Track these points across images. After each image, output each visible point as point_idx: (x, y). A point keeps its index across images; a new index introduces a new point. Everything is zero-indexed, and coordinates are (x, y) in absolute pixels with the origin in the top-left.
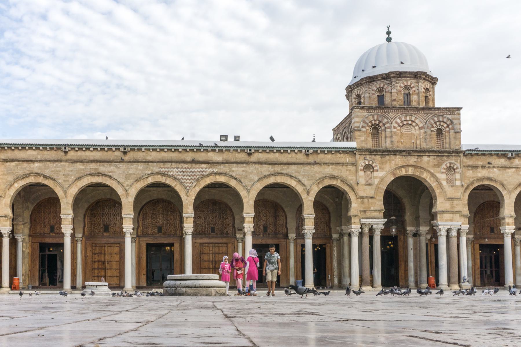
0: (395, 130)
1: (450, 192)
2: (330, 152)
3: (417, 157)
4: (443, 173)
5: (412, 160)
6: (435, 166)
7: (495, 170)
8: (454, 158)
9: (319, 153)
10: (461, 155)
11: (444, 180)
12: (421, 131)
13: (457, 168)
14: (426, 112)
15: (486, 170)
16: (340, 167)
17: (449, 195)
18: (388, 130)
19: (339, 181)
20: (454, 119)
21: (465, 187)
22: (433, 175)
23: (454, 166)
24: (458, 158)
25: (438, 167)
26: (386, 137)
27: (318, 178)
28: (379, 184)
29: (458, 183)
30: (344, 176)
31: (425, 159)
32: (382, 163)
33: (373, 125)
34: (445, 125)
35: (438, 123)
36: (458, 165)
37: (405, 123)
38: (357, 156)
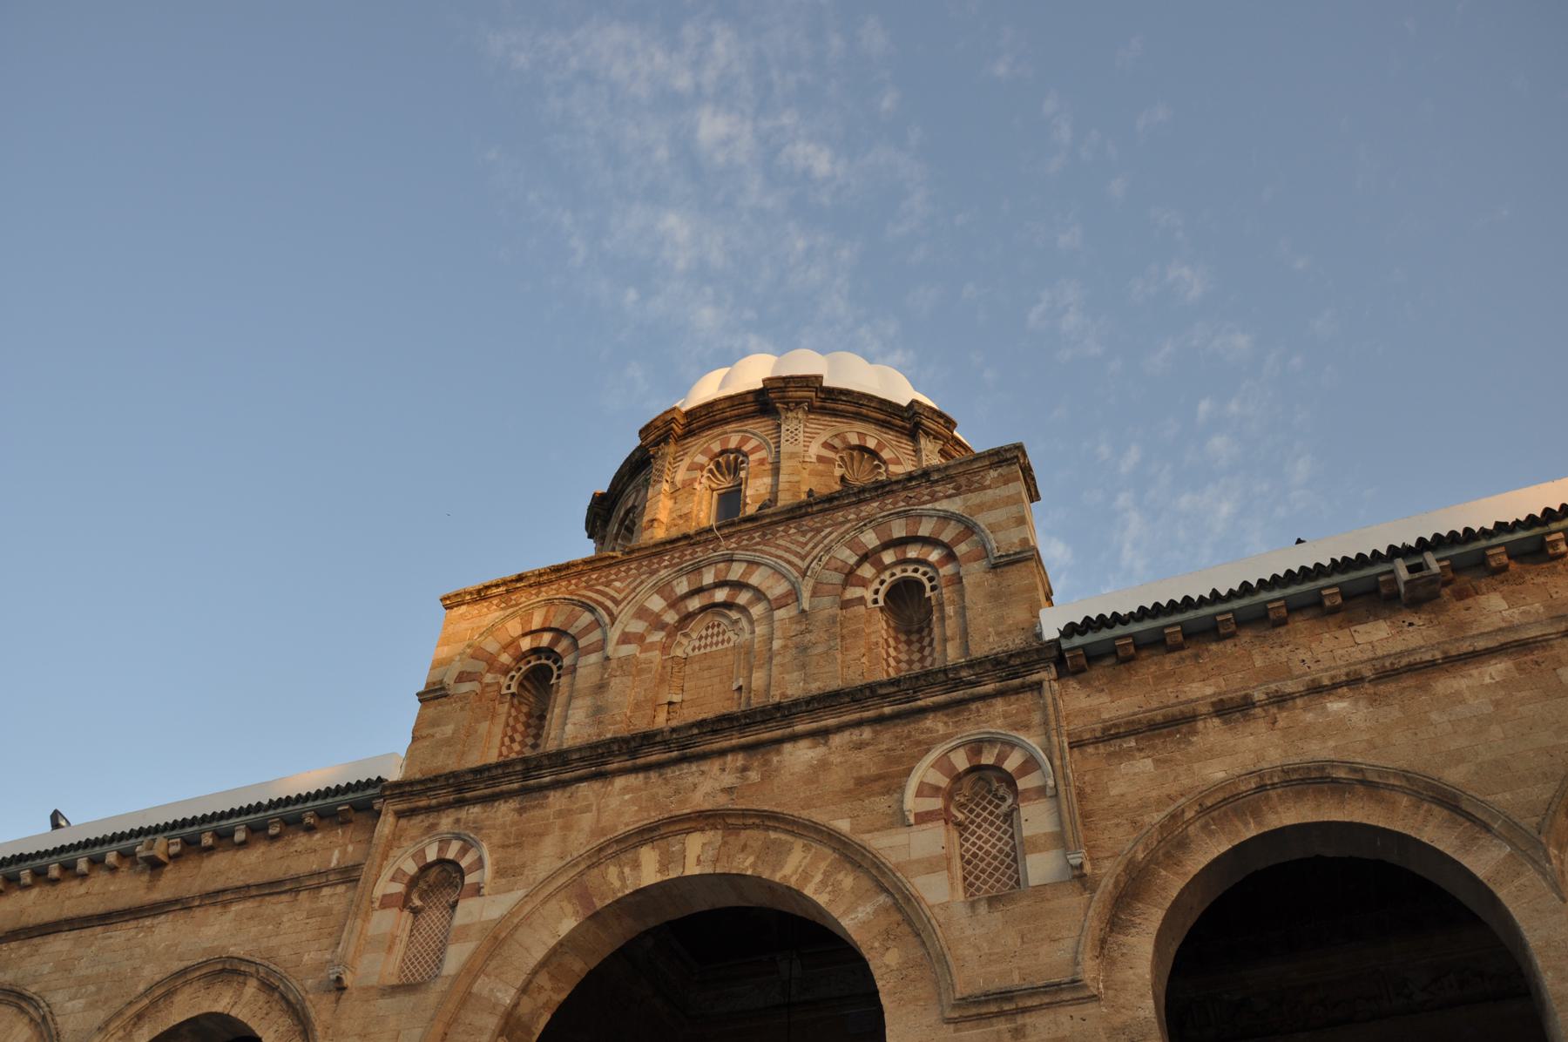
0: (630, 649)
1: (981, 947)
2: (258, 831)
3: (740, 760)
4: (923, 818)
5: (706, 784)
6: (862, 786)
7: (1336, 706)
8: (999, 705)
9: (210, 849)
10: (1046, 675)
11: (932, 865)
12: (780, 614)
13: (1030, 765)
14: (816, 522)
15: (1261, 726)
16: (277, 905)
17: (972, 976)
18: (594, 658)
19: (251, 988)
20: (981, 507)
21: (1107, 884)
22: (850, 853)
23: (1002, 757)
24: (1028, 699)
25: (888, 791)
26: (570, 698)
27: (141, 988)
28: (472, 971)
29: (1040, 867)
30: (285, 953)
31: (799, 756)
32: (519, 840)
33: (523, 656)
34: (934, 556)
35: (888, 557)
36: (1033, 741)
37: (694, 604)
38: (386, 825)
